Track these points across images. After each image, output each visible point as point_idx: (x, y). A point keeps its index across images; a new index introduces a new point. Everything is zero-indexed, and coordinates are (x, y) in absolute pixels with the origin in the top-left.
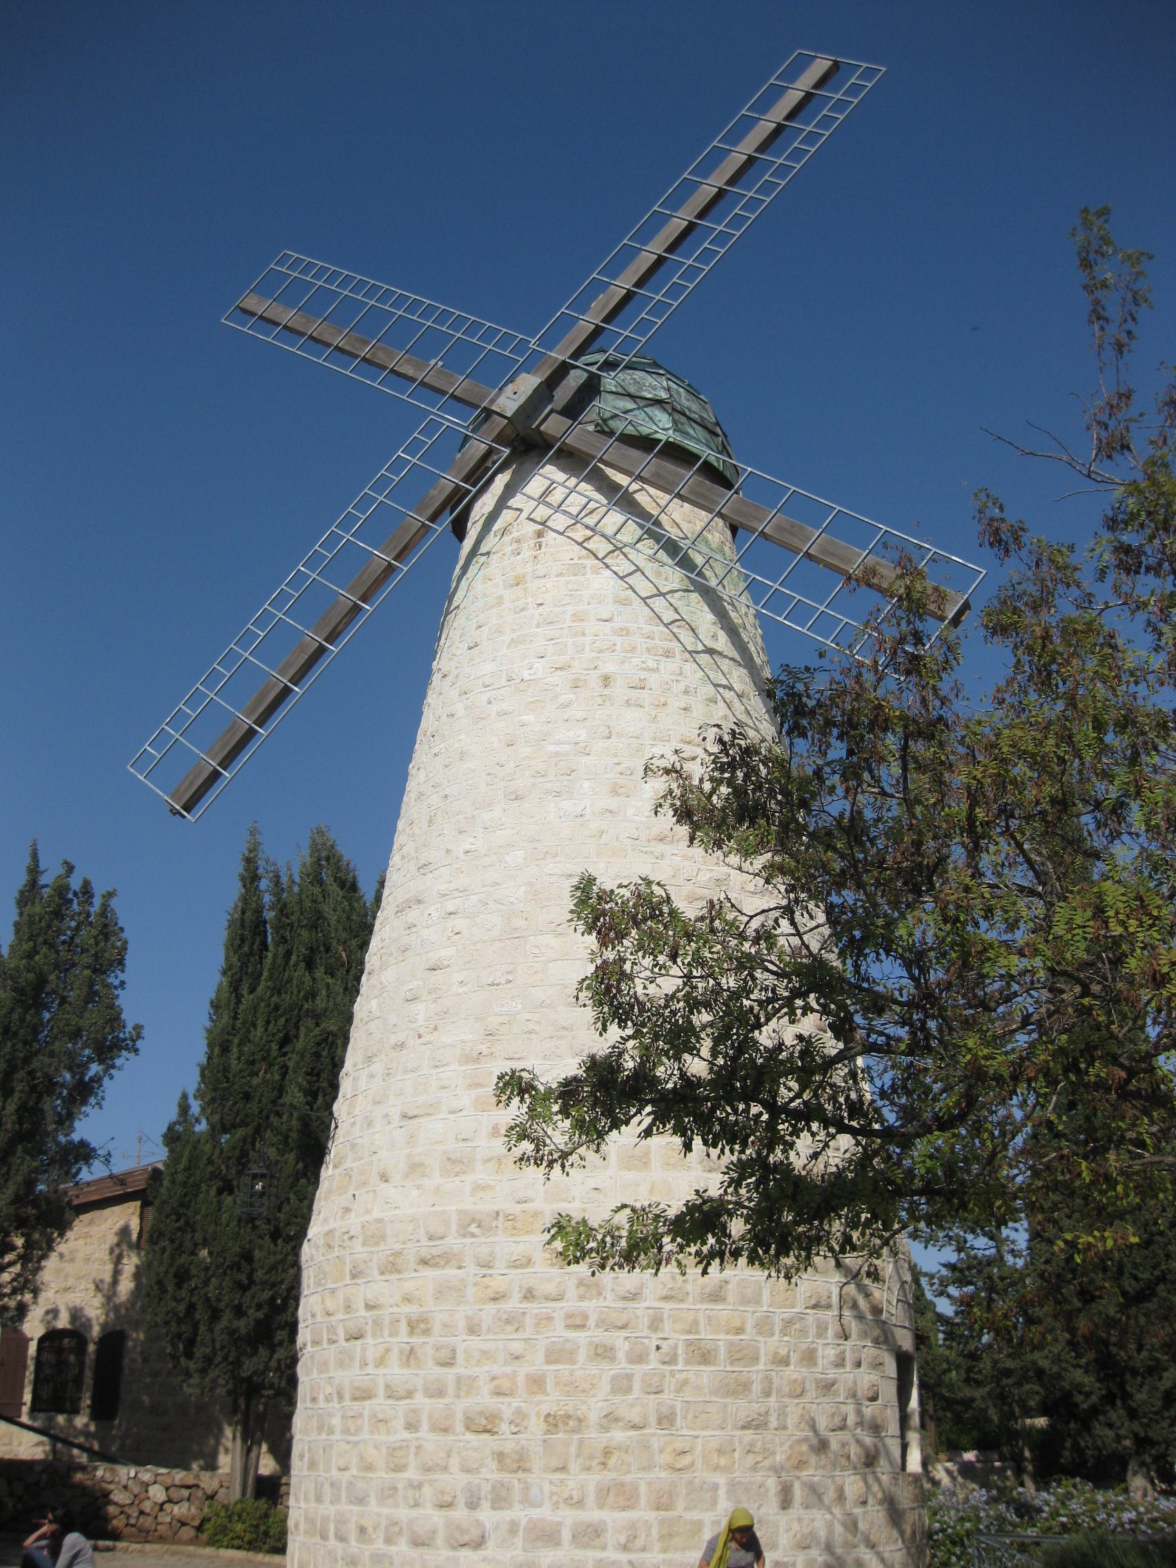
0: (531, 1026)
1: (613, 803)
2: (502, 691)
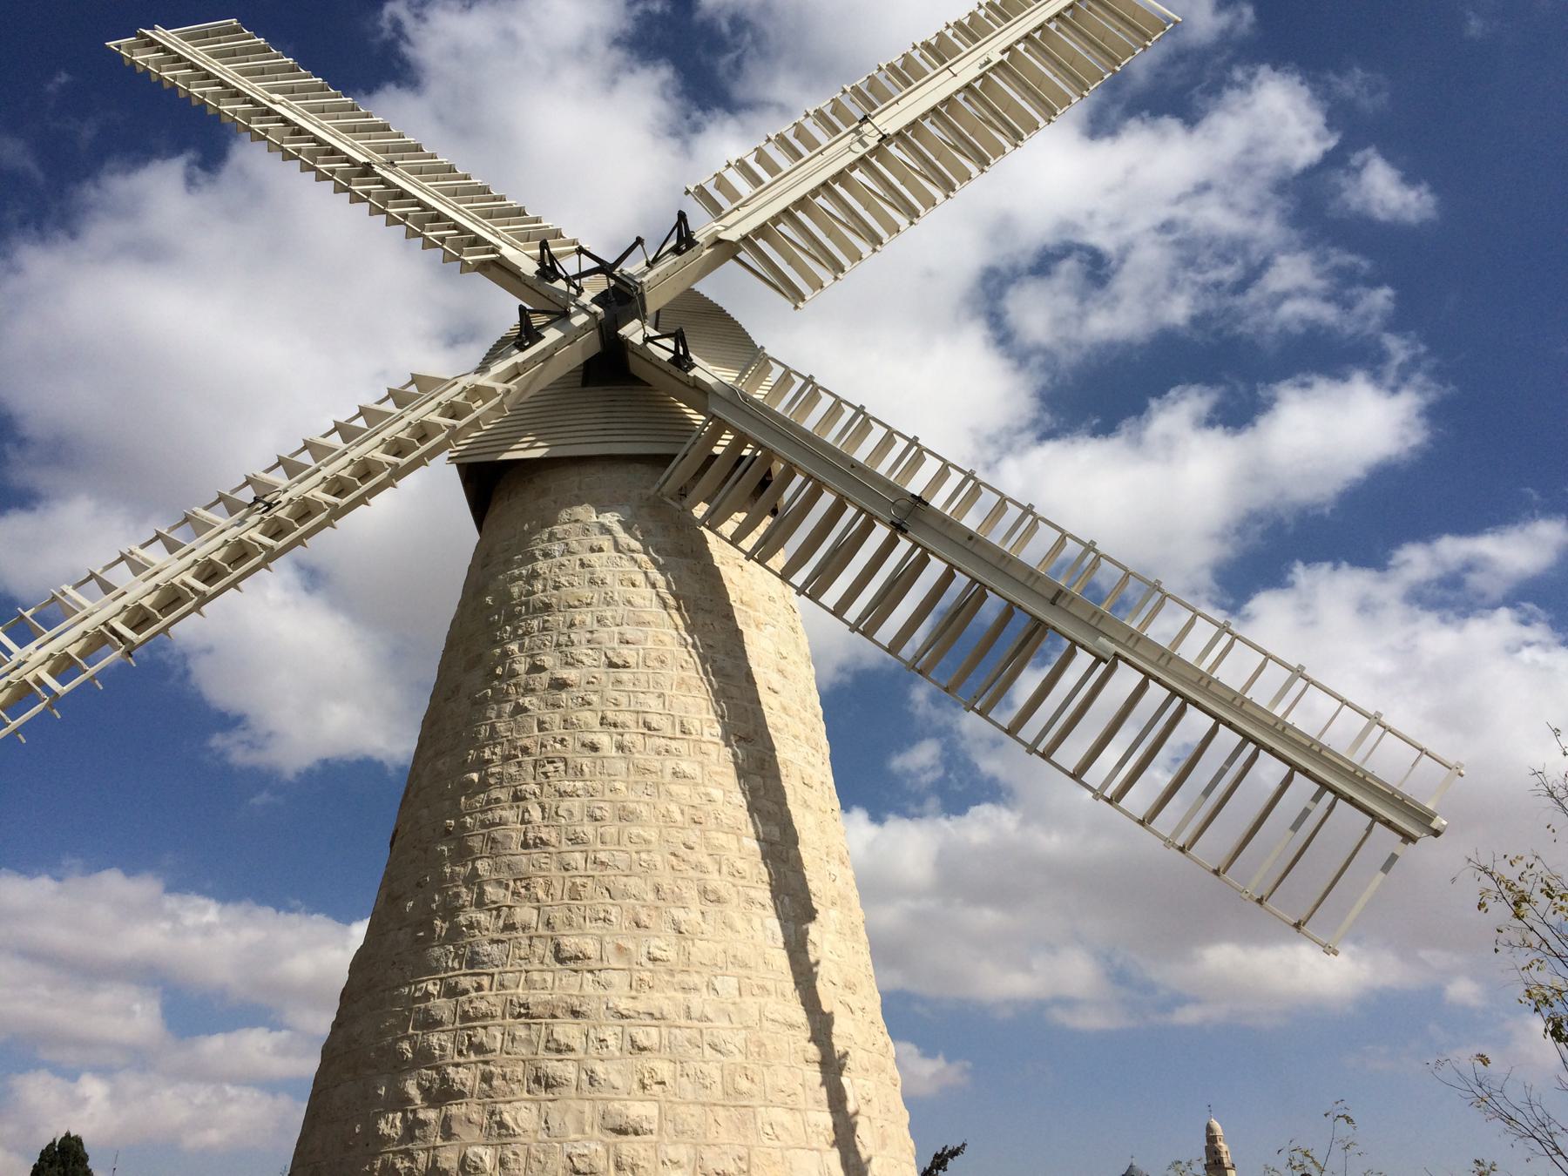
2: (673, 745)
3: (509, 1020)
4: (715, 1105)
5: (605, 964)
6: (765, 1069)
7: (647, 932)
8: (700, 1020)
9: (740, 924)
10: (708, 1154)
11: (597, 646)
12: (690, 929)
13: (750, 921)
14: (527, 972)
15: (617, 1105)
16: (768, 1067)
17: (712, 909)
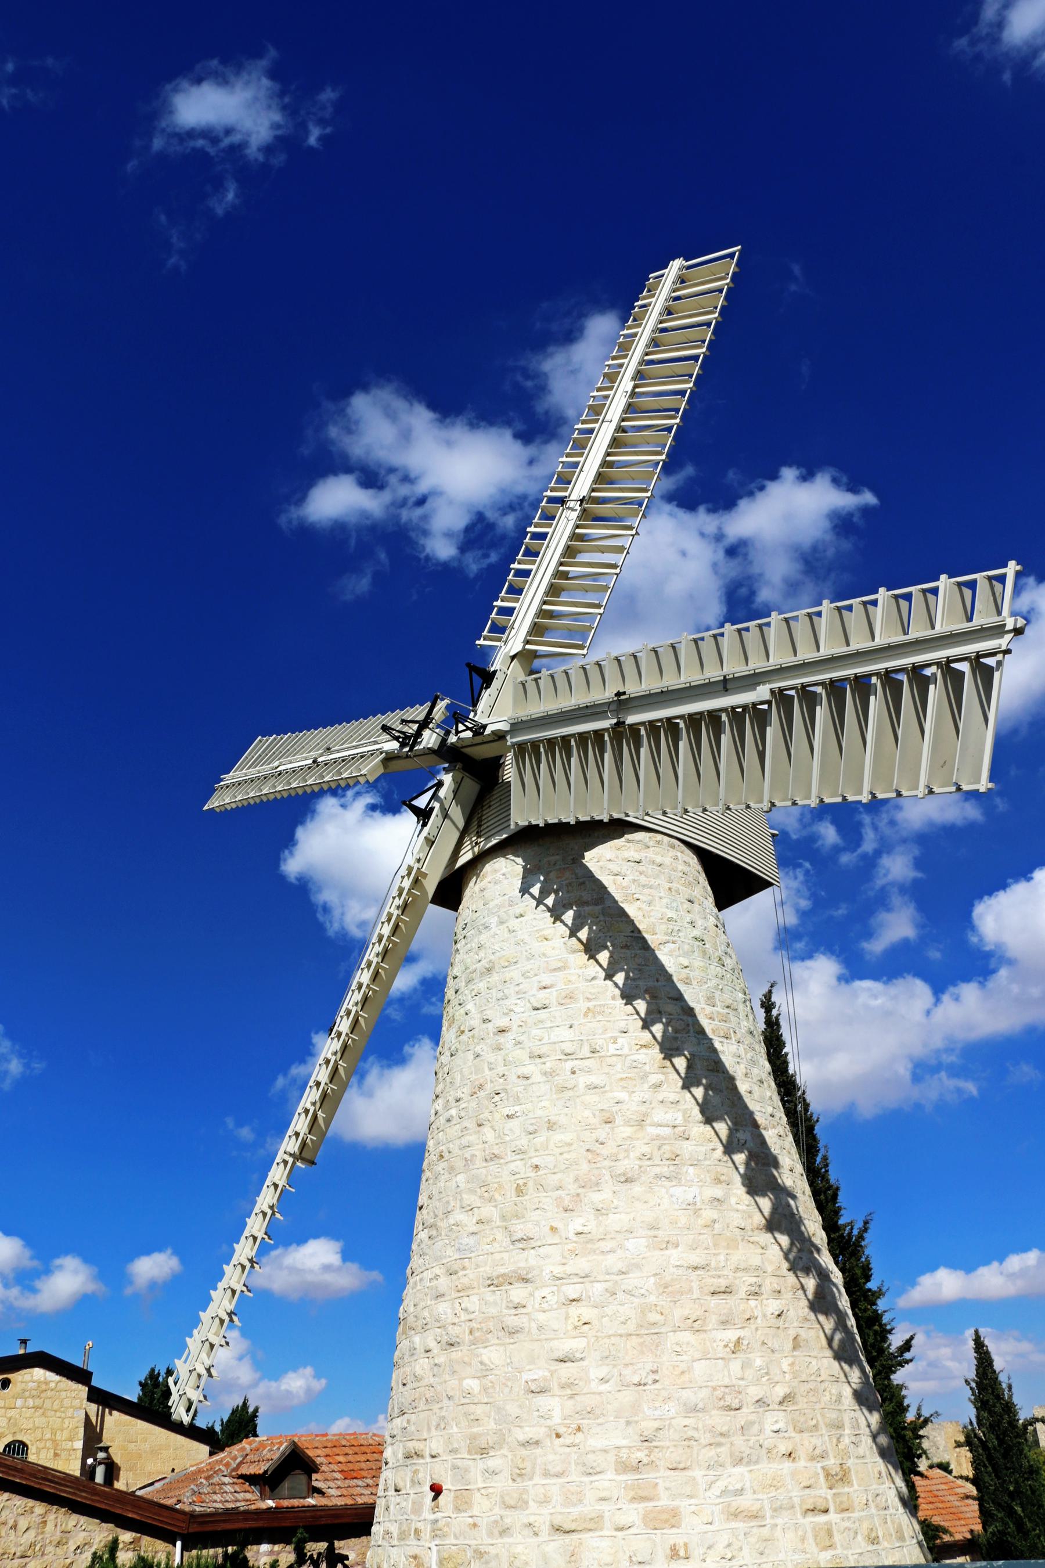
0: (690, 1433)
1: (718, 1192)
3: (483, 1290)
4: (630, 1335)
5: (544, 1242)
7: (573, 1214)
10: (627, 1372)
11: (523, 996)
12: (605, 1207)
14: (492, 1254)
15: (556, 1342)
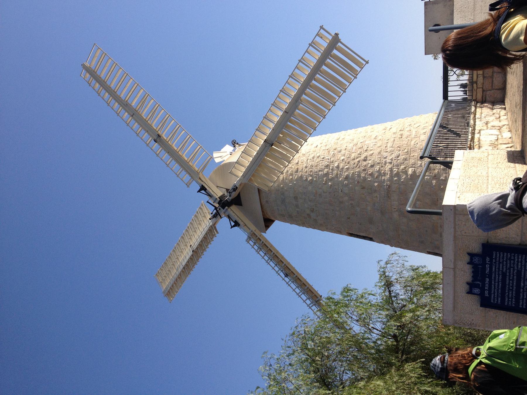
6: (403, 146)
8: (392, 160)
9: (372, 152)
13: (371, 150)
16: (402, 145)
17: (368, 158)
